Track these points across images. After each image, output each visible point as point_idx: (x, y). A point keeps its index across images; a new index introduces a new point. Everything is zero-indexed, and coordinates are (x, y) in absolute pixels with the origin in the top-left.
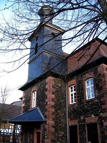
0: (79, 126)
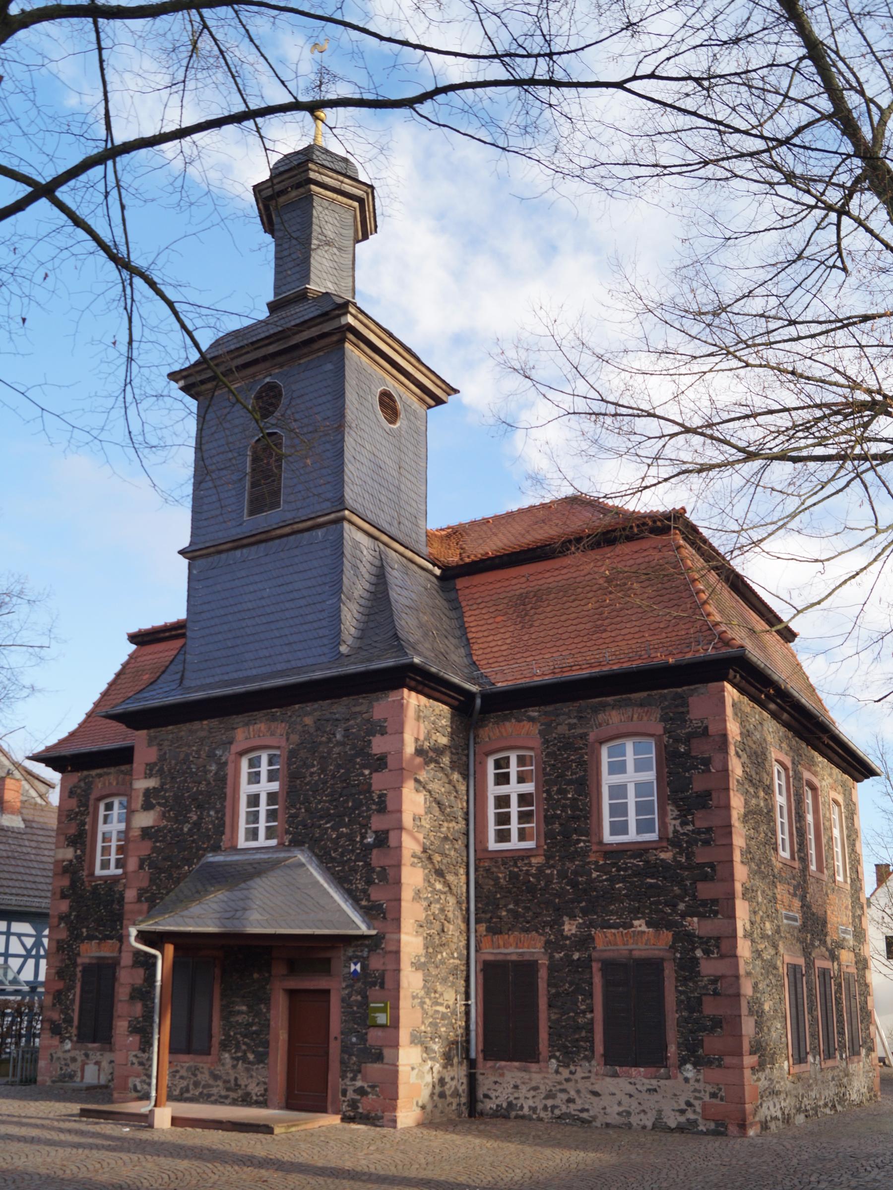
0: (552, 968)
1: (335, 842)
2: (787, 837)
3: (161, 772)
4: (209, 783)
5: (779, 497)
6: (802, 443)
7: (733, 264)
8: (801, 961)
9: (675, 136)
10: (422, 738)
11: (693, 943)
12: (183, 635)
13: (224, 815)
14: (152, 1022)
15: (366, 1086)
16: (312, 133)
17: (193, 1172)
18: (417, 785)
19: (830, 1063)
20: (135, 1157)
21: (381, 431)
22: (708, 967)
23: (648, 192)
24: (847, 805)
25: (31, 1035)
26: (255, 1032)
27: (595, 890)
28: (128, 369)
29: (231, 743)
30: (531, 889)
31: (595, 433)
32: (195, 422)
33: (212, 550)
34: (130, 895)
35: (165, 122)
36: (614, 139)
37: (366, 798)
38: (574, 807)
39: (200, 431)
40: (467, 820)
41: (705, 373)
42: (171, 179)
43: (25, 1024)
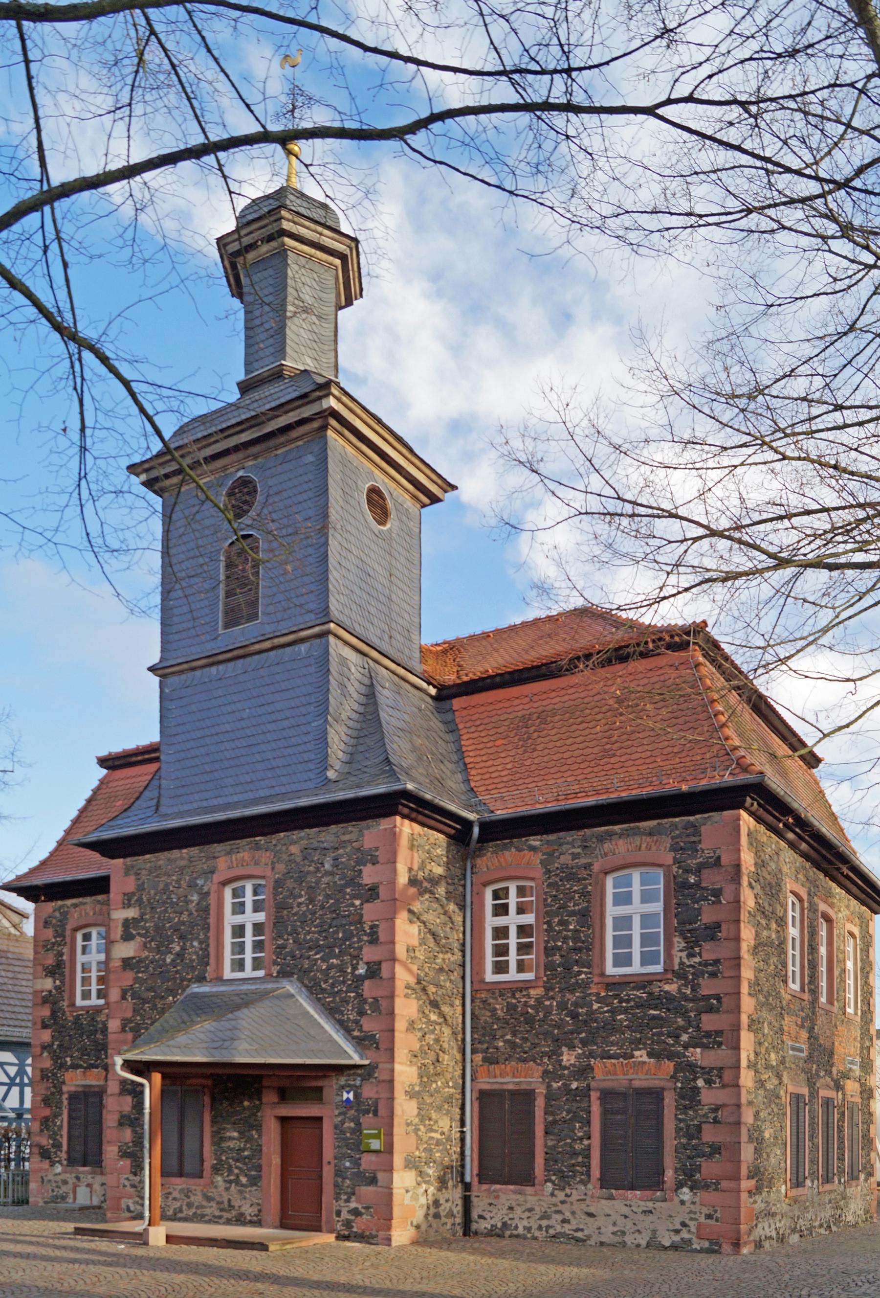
0: (550, 1097)
1: (326, 973)
2: (797, 969)
3: (140, 901)
4: (191, 914)
5: (811, 609)
6: (841, 548)
7: (774, 336)
8: (805, 1091)
9: (714, 176)
10: (415, 867)
11: (695, 1073)
12: (157, 759)
13: (208, 945)
14: (142, 1147)
15: (360, 1207)
16: (285, 172)
17: (190, 1286)
18: (411, 916)
19: (828, 1187)
20: (131, 1272)
21: (369, 533)
22: (708, 1097)
23: (680, 247)
24: (863, 938)
25: (20, 1159)
26: (246, 1157)
27: (596, 1021)
28: (82, 461)
29: (213, 872)
30: (530, 1021)
31: (609, 536)
32: (161, 522)
33: (185, 666)
34: (114, 1025)
35: (110, 157)
36: (642, 181)
37: (357, 929)
38: (576, 939)
39: (166, 532)
40: (463, 951)
41: (736, 467)
42: (121, 230)
43: (13, 1149)
